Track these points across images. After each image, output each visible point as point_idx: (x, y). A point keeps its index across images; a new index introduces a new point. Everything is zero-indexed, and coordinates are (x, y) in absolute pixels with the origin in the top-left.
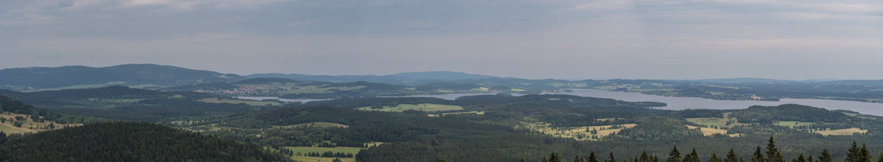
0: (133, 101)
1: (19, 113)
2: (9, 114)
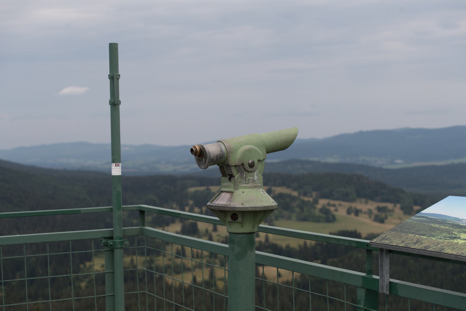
1: (383, 201)
2: (366, 203)
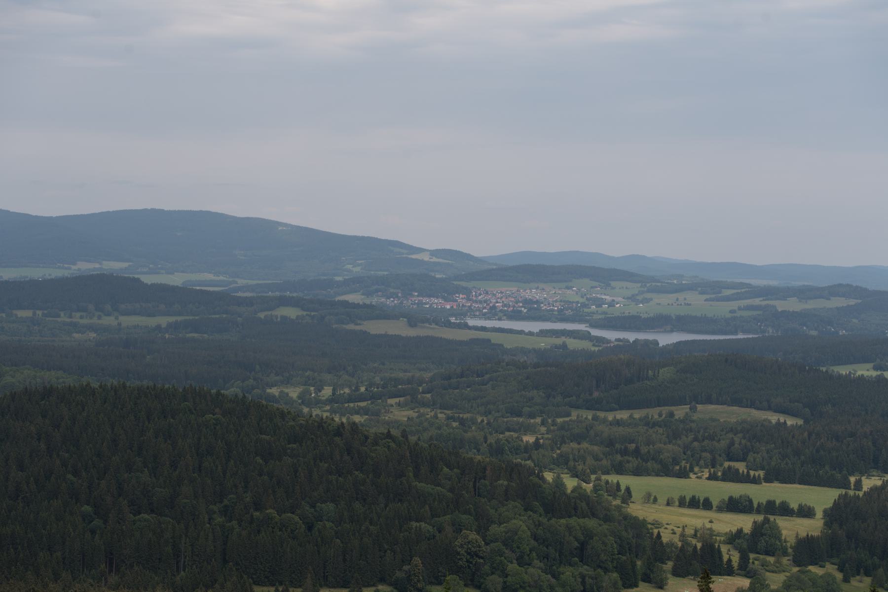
0: (152, 322)
